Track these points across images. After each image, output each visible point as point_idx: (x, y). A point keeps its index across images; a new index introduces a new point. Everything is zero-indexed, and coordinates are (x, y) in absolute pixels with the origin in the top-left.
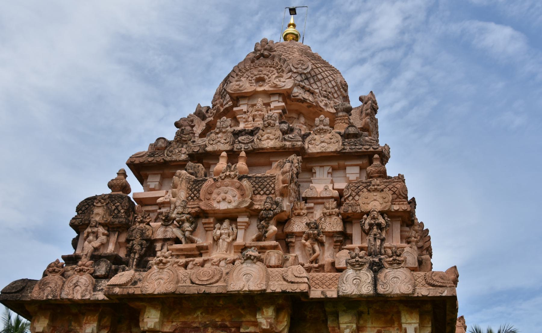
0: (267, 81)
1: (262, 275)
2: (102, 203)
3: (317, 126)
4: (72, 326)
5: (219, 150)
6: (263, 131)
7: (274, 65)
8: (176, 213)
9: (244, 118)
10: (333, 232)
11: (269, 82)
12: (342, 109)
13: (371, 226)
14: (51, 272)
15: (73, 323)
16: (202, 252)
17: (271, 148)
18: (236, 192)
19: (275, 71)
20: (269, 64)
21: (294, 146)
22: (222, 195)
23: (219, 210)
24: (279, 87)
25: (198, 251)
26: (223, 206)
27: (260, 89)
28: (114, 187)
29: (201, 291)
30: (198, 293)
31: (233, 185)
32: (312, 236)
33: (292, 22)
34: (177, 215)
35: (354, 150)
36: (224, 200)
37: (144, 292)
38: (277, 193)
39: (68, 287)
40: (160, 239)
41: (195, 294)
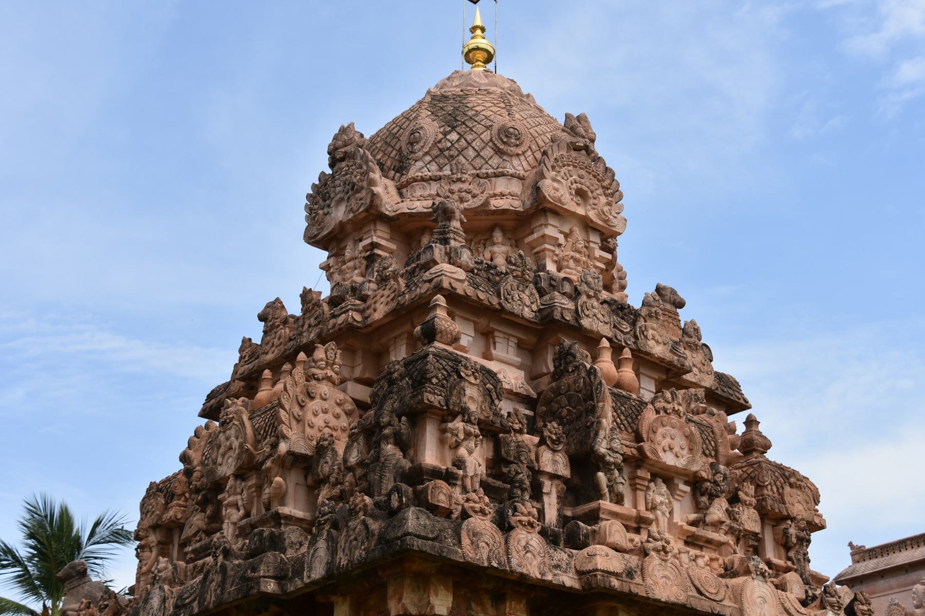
0: (592, 201)
1: (775, 603)
2: (476, 379)
3: (691, 337)
4: (473, 610)
5: (598, 332)
6: (645, 321)
7: (598, 175)
8: (605, 447)
9: (557, 255)
10: (750, 532)
11: (596, 207)
12: (672, 299)
13: (801, 541)
14: (476, 512)
15: (473, 605)
16: (643, 526)
17: (659, 358)
18: (684, 442)
19: (600, 191)
20: (593, 171)
21: (684, 366)
22: (668, 440)
23: (665, 463)
24: (611, 224)
25: (636, 523)
26: (669, 459)
27: (580, 211)
28: (444, 334)
29: (716, 610)
30: (713, 613)
31: (681, 428)
32: (737, 533)
33: (478, 23)
34: (607, 451)
35: (725, 395)
36: (671, 449)
37: (650, 595)
38: (721, 459)
39: (517, 552)
40: (548, 473)
41: (709, 613)
